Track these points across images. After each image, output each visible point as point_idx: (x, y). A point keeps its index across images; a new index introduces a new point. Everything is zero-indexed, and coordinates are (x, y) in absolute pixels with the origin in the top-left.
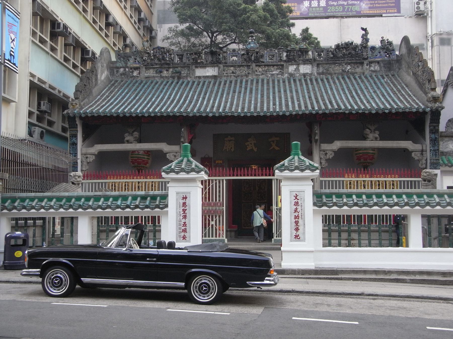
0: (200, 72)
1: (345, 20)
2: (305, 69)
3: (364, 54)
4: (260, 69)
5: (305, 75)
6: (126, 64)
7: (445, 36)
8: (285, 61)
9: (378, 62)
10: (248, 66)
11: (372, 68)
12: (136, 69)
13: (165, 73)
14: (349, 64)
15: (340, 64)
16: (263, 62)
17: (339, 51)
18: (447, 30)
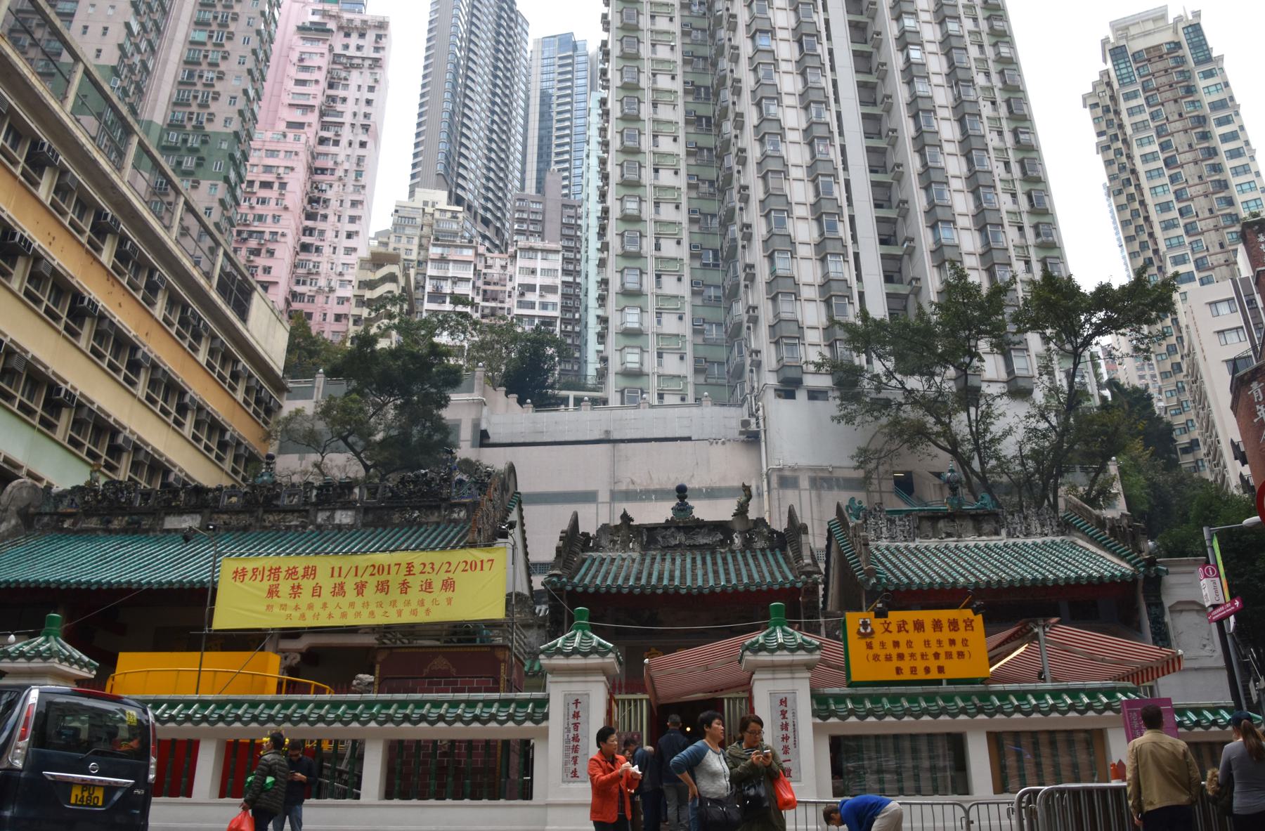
0: (171, 522)
1: (622, 445)
2: (344, 517)
3: (445, 491)
4: (271, 518)
5: (340, 527)
6: (56, 507)
7: (787, 473)
8: (315, 505)
9: (464, 505)
10: (251, 513)
11: (455, 515)
12: (70, 515)
13: (116, 524)
14: (419, 508)
15: (402, 509)
16: (277, 506)
17: (405, 486)
18: (791, 462)
